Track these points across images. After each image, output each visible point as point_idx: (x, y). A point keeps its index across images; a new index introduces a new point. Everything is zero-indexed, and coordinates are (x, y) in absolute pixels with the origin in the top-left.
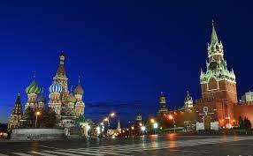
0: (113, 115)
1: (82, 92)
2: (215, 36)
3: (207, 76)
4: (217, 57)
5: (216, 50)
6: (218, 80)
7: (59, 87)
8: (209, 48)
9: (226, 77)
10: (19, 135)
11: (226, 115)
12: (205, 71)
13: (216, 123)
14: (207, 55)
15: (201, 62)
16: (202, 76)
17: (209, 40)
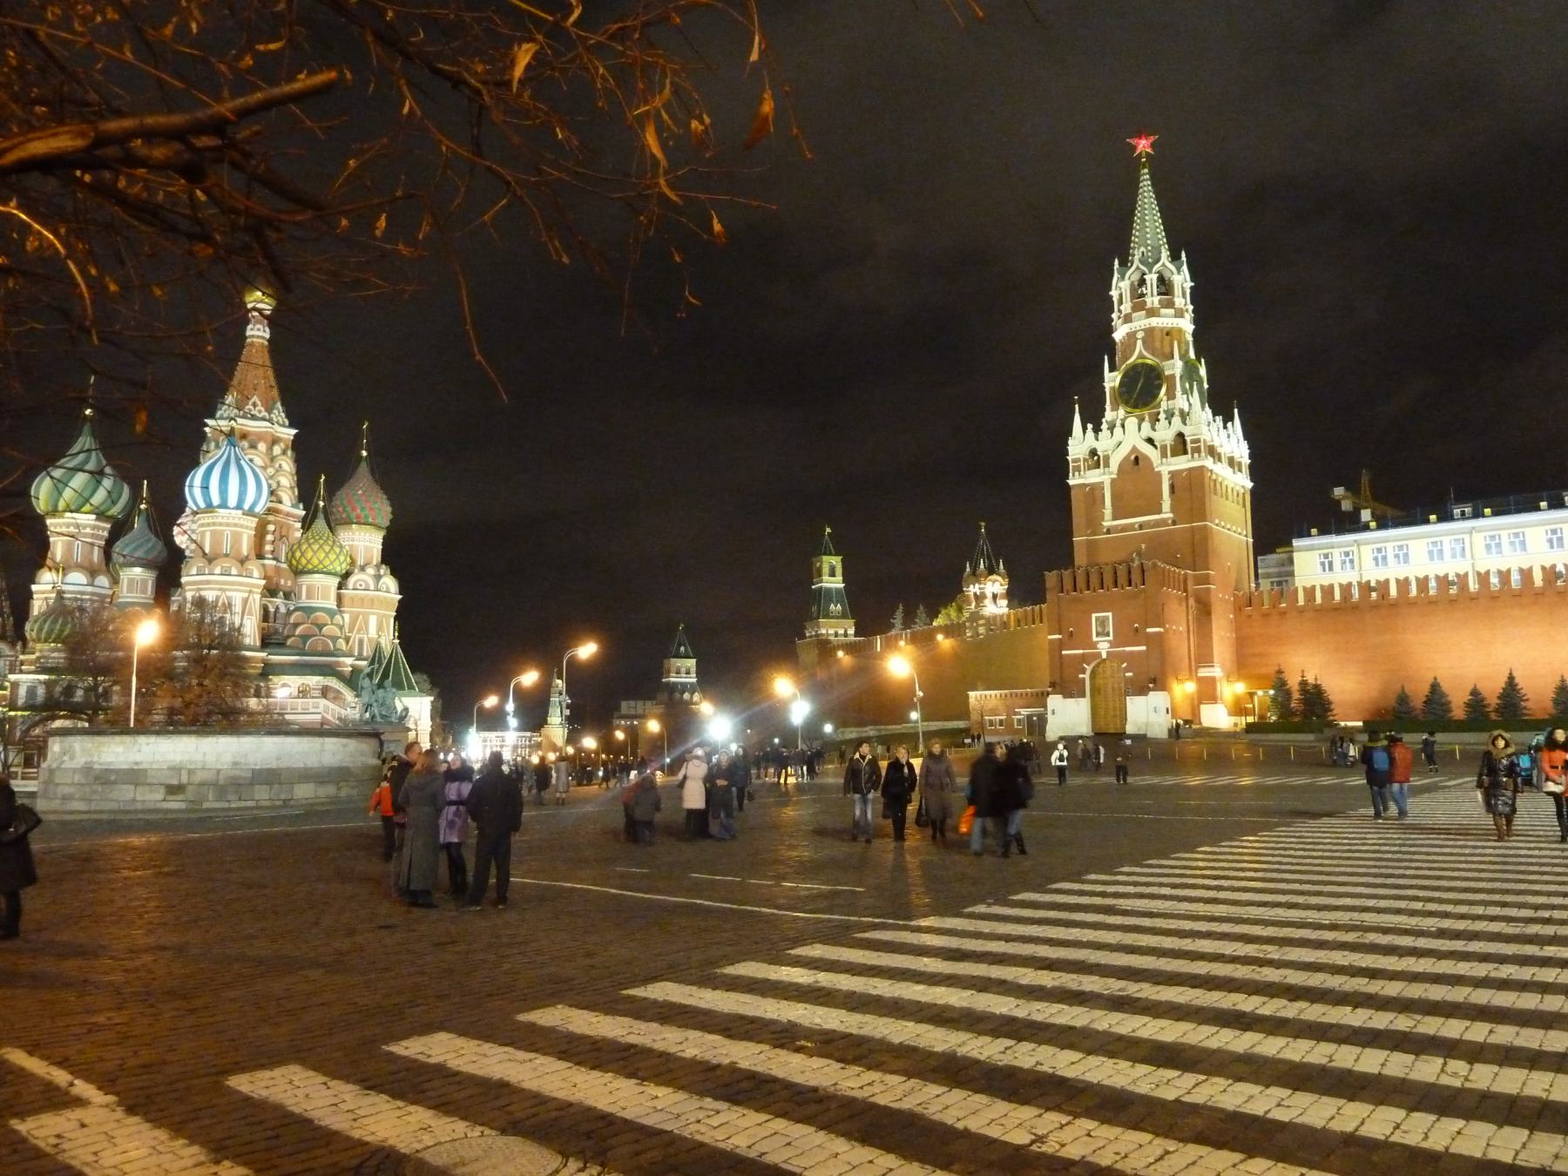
0: (587, 651)
1: (383, 511)
2: (1149, 222)
3: (1104, 443)
4: (1159, 340)
5: (1153, 304)
6: (1168, 467)
7: (243, 478)
8: (1120, 287)
9: (1212, 451)
10: (104, 778)
11: (1205, 658)
12: (1094, 418)
13: (1157, 699)
14: (1111, 330)
15: (1074, 366)
16: (1079, 443)
17: (1116, 243)
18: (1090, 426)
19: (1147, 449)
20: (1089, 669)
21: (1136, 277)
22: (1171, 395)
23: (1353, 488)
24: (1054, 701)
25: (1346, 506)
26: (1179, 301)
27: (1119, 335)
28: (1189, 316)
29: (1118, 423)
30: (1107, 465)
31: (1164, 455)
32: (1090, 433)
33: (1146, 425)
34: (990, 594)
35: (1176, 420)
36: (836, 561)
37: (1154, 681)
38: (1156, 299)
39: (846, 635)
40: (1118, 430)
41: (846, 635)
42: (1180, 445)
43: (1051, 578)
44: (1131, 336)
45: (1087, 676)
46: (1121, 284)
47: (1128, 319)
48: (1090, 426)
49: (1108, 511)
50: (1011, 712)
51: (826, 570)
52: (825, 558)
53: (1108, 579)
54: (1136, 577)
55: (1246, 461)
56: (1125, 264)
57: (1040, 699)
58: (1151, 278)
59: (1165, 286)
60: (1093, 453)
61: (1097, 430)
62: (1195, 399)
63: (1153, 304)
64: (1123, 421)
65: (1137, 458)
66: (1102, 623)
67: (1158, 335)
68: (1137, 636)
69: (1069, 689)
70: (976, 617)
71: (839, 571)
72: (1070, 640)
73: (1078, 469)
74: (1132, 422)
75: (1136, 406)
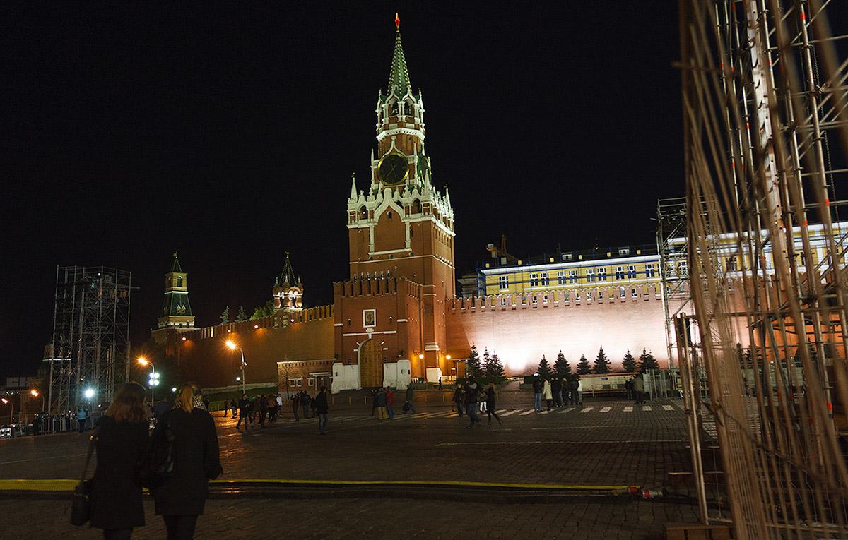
2: (400, 71)
3: (370, 203)
5: (403, 121)
8: (382, 107)
9: (435, 212)
12: (364, 187)
13: (403, 364)
15: (352, 155)
17: (382, 82)
18: (362, 192)
19: (397, 208)
20: (360, 345)
21: (391, 102)
22: (412, 176)
23: (498, 246)
24: (337, 367)
25: (494, 255)
26: (417, 120)
27: (380, 137)
28: (422, 130)
29: (380, 191)
30: (372, 217)
31: (407, 213)
32: (362, 197)
33: (397, 193)
34: (292, 297)
35: (415, 191)
36: (183, 276)
37: (401, 353)
38: (404, 117)
39: (188, 326)
40: (379, 195)
41: (188, 326)
42: (417, 207)
43: (337, 286)
44: (388, 138)
45: (358, 350)
46: (383, 106)
47: (386, 128)
48: (362, 192)
49: (372, 246)
50: (306, 375)
51: (175, 281)
52: (175, 274)
53: (382, 287)
54: (391, 287)
55: (452, 220)
56: (385, 94)
57: (328, 367)
58: (402, 103)
59: (409, 109)
60: (364, 208)
61: (366, 195)
62: (427, 181)
63: (403, 121)
64: (383, 190)
65: (390, 213)
66: (370, 316)
67: (404, 138)
68: (391, 324)
69: (348, 360)
70: (282, 313)
71: (184, 282)
72: (349, 327)
73: (354, 218)
74: (388, 191)
75: (390, 182)
